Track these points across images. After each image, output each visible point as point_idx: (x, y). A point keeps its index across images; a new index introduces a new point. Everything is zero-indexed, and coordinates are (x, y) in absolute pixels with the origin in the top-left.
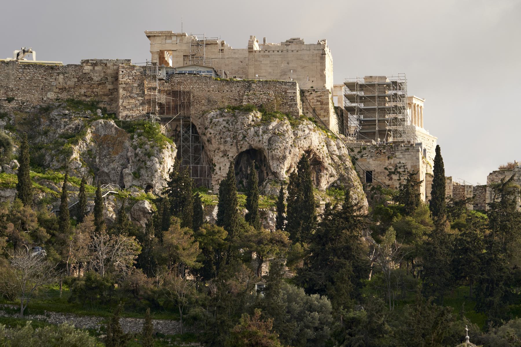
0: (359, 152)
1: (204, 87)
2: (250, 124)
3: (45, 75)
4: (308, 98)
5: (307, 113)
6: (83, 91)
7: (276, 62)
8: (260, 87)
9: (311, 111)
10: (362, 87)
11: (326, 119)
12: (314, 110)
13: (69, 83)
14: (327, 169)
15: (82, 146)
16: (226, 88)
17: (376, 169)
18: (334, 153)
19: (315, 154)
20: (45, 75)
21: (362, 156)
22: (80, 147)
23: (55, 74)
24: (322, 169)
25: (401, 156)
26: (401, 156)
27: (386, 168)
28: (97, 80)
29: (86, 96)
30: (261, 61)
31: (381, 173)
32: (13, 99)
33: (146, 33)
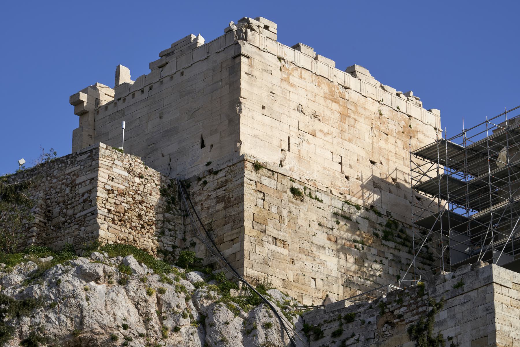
4: (198, 199)
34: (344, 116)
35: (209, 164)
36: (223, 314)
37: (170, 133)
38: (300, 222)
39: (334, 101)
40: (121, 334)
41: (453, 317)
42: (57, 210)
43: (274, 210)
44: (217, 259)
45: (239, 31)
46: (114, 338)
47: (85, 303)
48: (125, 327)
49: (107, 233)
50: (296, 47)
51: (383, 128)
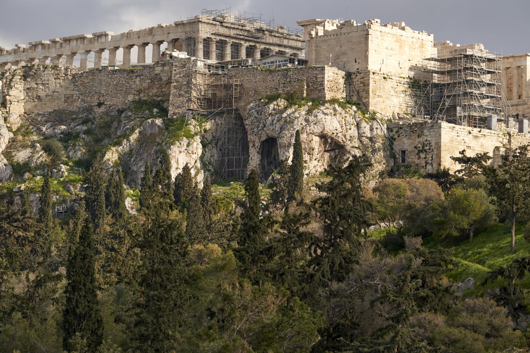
0: (397, 132)
1: (252, 78)
2: (271, 113)
3: (127, 79)
4: (354, 80)
5: (353, 96)
6: (155, 91)
7: (332, 46)
8: (296, 74)
9: (356, 93)
10: (450, 60)
11: (367, 100)
12: (358, 92)
13: (144, 84)
14: (350, 152)
15: (125, 146)
16: (269, 77)
17: (408, 148)
18: (363, 135)
19: (332, 139)
20: (127, 79)
21: (399, 136)
22: (123, 148)
23: (134, 77)
24: (345, 153)
25: (428, 133)
26: (428, 133)
27: (416, 147)
28: (165, 79)
29: (156, 96)
30: (321, 47)
31: (412, 151)
32: (103, 104)
33: (299, 23)
34: (400, 46)
35: (358, 69)
36: (364, 124)
37: (344, 54)
38: (386, 88)
39: (398, 42)
40: (335, 132)
41: (430, 135)
42: (311, 85)
43: (378, 86)
44: (361, 102)
45: (368, 25)
46: (333, 134)
47: (325, 123)
48: (336, 130)
49: (328, 97)
50: (386, 26)
51: (413, 47)
